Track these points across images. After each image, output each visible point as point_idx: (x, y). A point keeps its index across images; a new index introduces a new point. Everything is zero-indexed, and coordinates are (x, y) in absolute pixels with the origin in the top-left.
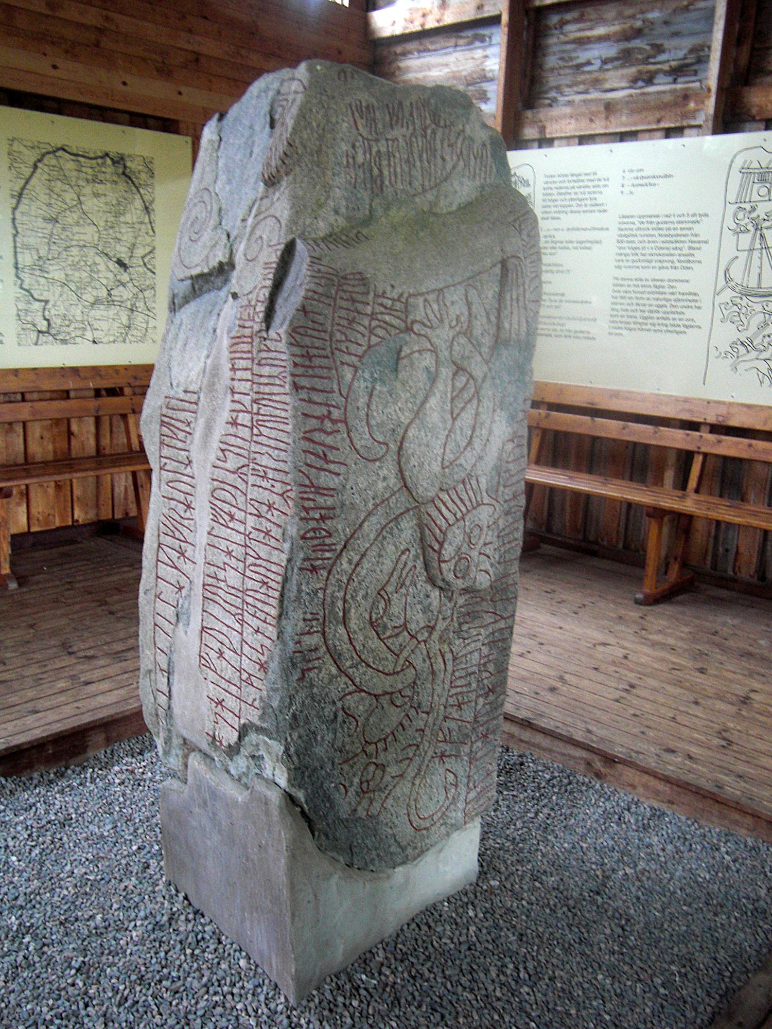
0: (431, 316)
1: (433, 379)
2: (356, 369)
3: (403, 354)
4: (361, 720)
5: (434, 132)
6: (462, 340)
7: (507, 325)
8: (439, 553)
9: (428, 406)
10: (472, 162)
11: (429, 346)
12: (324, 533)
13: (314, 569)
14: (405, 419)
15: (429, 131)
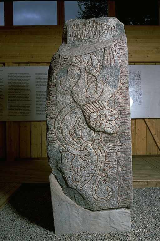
0: (78, 61)
1: (80, 76)
2: (57, 74)
3: (69, 70)
4: (69, 160)
5: (96, 26)
6: (89, 66)
7: (106, 63)
8: (89, 119)
9: (79, 82)
10: (110, 30)
11: (77, 68)
12: (52, 110)
13: (51, 118)
14: (72, 85)
15: (95, 26)
